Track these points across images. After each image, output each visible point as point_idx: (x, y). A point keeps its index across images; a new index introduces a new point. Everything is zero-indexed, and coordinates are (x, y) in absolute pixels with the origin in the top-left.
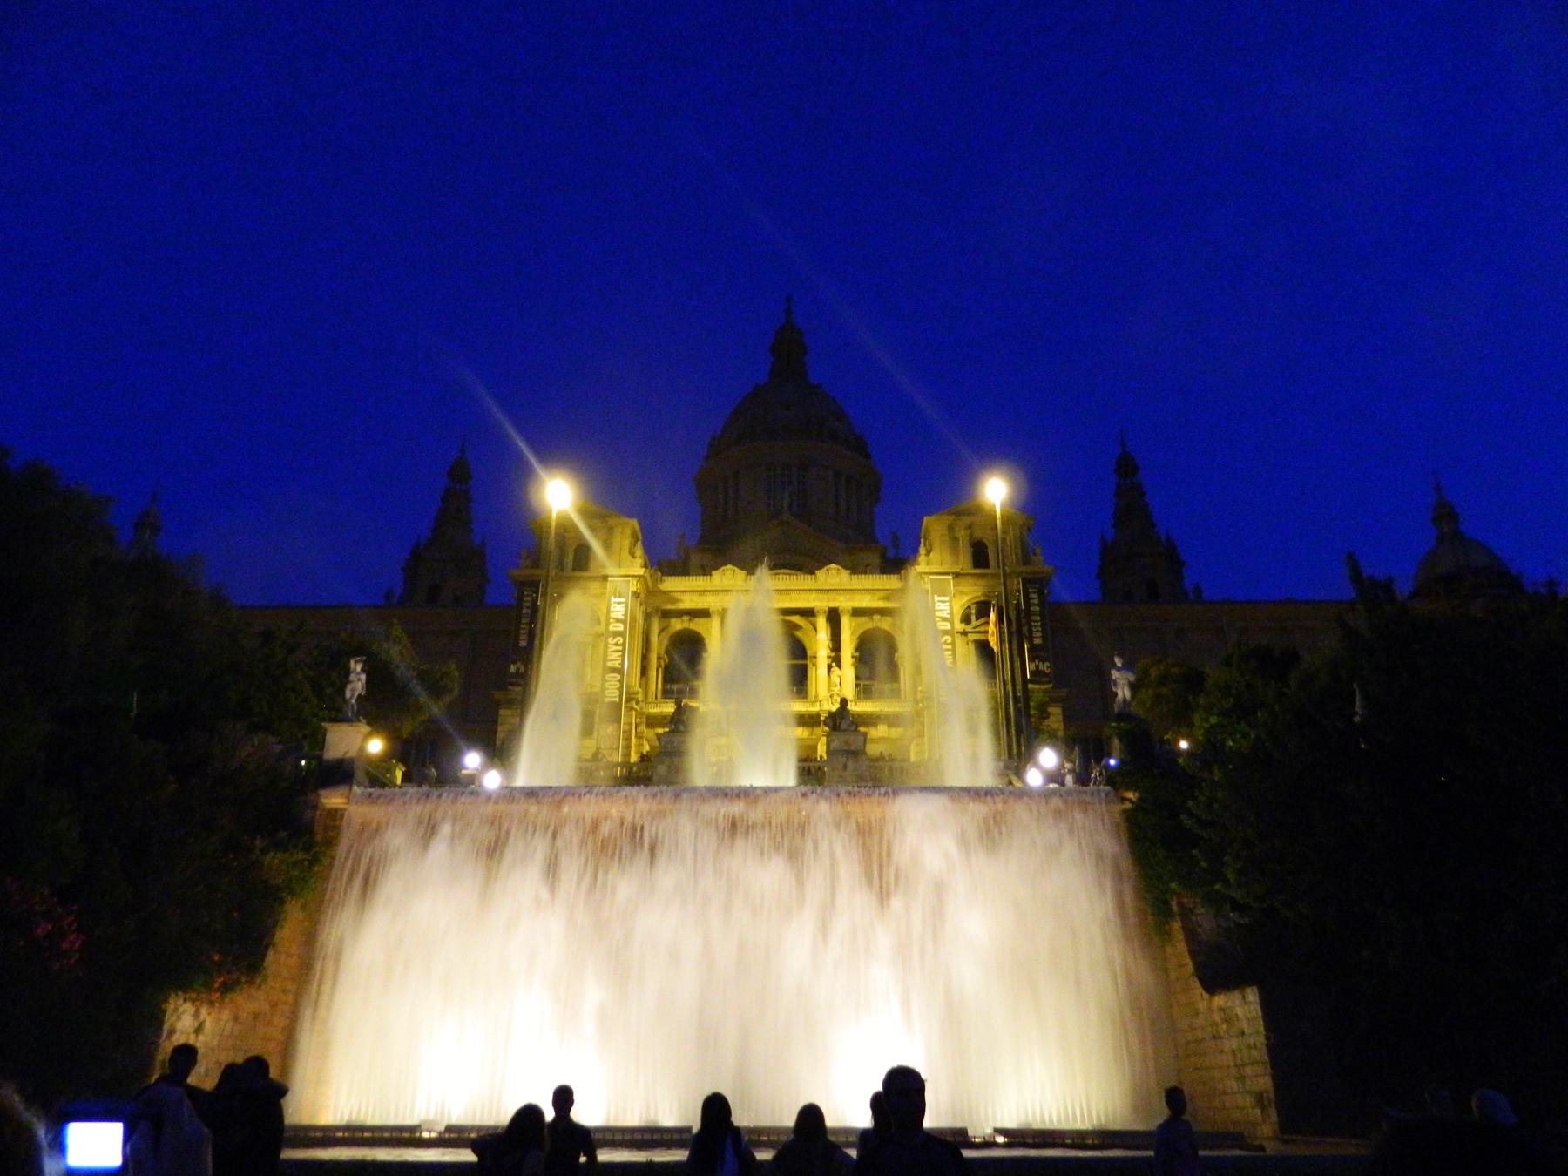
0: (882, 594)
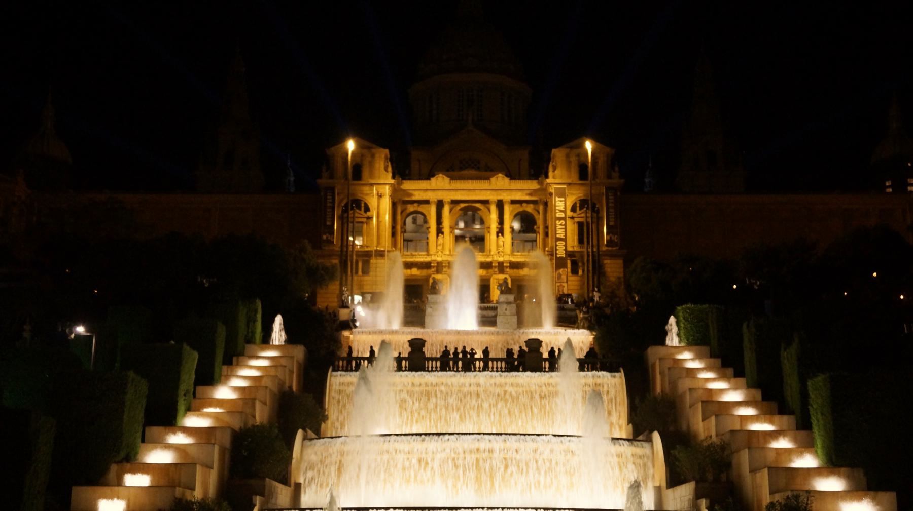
0: (528, 192)
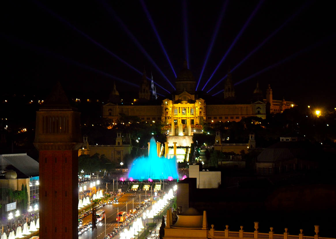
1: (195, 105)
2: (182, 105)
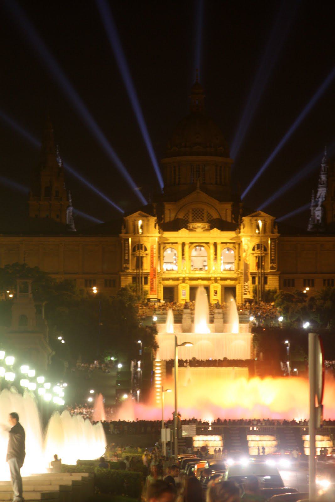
0: (231, 238)
1: (241, 234)
2: (192, 234)
